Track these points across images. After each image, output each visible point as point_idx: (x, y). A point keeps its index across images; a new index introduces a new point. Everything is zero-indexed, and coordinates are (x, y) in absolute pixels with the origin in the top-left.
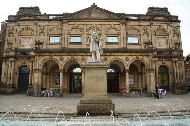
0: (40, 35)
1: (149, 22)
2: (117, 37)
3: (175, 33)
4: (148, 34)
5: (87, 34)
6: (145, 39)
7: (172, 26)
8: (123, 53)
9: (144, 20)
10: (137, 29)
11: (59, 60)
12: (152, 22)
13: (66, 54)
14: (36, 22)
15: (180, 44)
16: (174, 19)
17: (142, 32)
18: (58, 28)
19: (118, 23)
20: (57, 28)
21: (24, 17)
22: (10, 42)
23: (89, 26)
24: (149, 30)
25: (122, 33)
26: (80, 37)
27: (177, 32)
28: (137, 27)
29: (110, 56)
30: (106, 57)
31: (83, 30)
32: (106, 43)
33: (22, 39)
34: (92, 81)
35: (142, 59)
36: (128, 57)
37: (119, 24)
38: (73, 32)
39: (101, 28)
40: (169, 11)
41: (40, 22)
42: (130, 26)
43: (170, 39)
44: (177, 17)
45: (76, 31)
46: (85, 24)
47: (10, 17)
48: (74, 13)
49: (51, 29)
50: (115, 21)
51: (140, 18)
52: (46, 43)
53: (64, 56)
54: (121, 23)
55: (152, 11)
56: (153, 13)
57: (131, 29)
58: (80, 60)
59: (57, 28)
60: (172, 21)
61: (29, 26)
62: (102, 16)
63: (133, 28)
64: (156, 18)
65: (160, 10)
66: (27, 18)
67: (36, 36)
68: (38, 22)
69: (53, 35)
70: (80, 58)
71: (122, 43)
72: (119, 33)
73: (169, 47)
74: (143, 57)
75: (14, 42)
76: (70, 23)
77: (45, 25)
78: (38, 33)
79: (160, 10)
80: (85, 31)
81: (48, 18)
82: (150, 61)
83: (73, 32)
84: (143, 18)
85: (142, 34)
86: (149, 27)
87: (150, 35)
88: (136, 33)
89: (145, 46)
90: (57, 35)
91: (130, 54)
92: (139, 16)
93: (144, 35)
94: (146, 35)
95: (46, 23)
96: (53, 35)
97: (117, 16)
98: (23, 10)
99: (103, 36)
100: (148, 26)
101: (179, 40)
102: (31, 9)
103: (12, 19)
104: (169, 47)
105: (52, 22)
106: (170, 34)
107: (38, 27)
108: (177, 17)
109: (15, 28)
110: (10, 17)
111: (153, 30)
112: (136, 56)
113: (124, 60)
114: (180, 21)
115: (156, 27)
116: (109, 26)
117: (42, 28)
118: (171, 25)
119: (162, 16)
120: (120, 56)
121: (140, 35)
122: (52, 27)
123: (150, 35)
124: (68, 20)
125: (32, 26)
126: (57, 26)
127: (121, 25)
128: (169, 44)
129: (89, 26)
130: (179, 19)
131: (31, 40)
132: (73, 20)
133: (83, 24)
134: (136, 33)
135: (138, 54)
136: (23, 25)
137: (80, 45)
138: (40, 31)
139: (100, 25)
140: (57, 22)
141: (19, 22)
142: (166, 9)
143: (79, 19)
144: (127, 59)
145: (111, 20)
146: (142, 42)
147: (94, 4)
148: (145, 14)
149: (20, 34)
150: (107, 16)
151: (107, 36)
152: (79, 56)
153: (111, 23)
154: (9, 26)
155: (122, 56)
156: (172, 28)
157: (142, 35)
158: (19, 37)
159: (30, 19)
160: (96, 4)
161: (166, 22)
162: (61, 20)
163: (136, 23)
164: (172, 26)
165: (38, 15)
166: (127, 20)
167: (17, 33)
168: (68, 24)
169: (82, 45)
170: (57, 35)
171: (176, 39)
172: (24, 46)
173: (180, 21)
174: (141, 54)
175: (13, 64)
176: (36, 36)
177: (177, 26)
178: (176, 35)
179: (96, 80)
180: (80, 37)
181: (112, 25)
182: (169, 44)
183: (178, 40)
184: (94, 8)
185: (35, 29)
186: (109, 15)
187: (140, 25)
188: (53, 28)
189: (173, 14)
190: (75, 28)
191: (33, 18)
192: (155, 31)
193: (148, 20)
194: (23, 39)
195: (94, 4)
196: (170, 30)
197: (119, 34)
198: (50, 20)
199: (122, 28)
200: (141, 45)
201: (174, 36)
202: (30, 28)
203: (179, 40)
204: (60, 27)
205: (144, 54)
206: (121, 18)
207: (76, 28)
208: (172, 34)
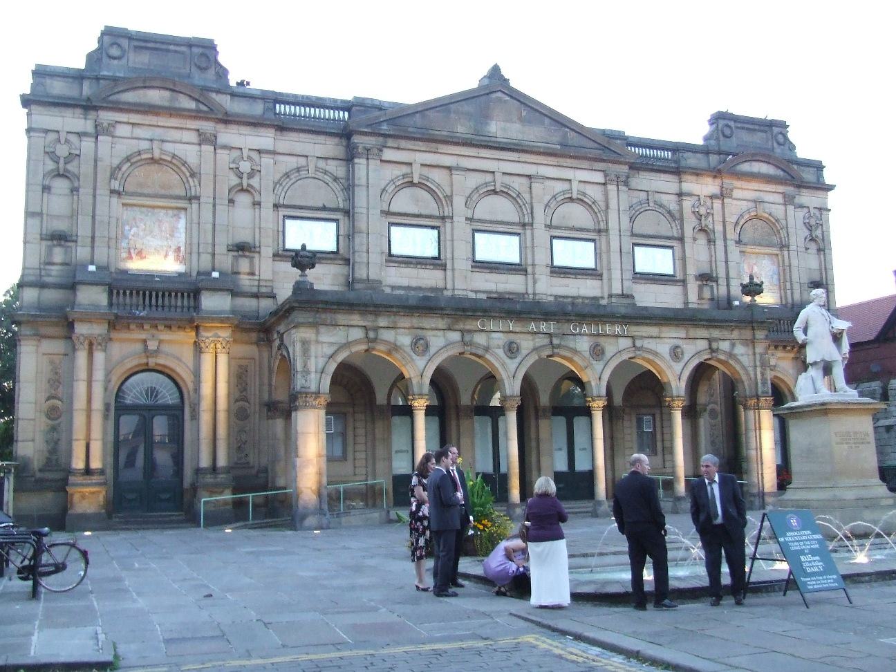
0: (231, 201)
1: (718, 181)
2: (593, 240)
3: (812, 240)
4: (712, 236)
5: (467, 219)
6: (698, 254)
7: (801, 206)
8: (664, 329)
9: (697, 173)
10: (669, 212)
11: (408, 349)
12: (728, 182)
13: (441, 323)
14: (207, 126)
15: (830, 288)
16: (808, 175)
17: (690, 223)
18: (325, 172)
19: (599, 178)
20: (320, 175)
21: (141, 92)
22: (61, 226)
23: (474, 180)
24: (718, 218)
25: (613, 224)
26: (436, 232)
27: (818, 233)
28: (670, 202)
29: (618, 336)
30: (602, 341)
31: (449, 198)
32: (549, 269)
33: (127, 214)
34: (846, 446)
35: (731, 355)
36: (680, 342)
37: (602, 181)
38: (404, 202)
39: (527, 196)
40: (792, 136)
41: (233, 129)
42: (643, 196)
43: (794, 262)
44: (818, 167)
45: (416, 201)
46: (458, 168)
47: (40, 73)
48: (416, 105)
49: (287, 175)
50: (586, 164)
51: (673, 160)
52: (267, 252)
53: (430, 333)
54: (613, 177)
55: (727, 132)
56: (734, 139)
57: (646, 207)
58: (500, 352)
59: (320, 175)
60: (801, 185)
61: (169, 147)
62: (533, 134)
63: (661, 206)
64: (745, 167)
65: (757, 127)
66: (155, 96)
67: (214, 206)
68: (220, 127)
69: (301, 208)
70: (501, 343)
71: (616, 274)
72: (602, 226)
73: (790, 300)
74: (733, 345)
75: (84, 231)
76: (388, 154)
77: (259, 151)
78: (224, 193)
79: (757, 127)
80: (459, 201)
81: (274, 113)
82: (758, 363)
83: (404, 202)
84: (692, 160)
85: (688, 233)
86: (717, 204)
87: (720, 243)
88: (665, 228)
89: (700, 288)
90: (324, 208)
91: (687, 333)
92: (676, 148)
93: (695, 239)
94: (702, 240)
95: (265, 139)
96: (301, 208)
97: (596, 145)
98: (125, 43)
99: (536, 233)
100: (711, 197)
101: (826, 269)
102: (172, 47)
103: (58, 88)
104: (790, 300)
105: (293, 136)
106: (792, 240)
107: (223, 156)
108: (818, 167)
109: (87, 145)
110: (40, 73)
111: (731, 219)
112: (710, 341)
113: (667, 357)
114: (830, 188)
115: (744, 205)
116: (559, 187)
117: (245, 167)
118: (798, 200)
119: (766, 158)
120: (650, 340)
121: (681, 239)
122: (293, 162)
123: (720, 243)
124: (381, 139)
125: (181, 141)
126: (321, 164)
127: (612, 188)
128: (788, 285)
129: (474, 180)
130: (828, 178)
131: (182, 224)
132: (403, 143)
133: (449, 168)
134: (665, 228)
135: (716, 333)
136: (129, 135)
137: (438, 274)
138: (234, 180)
139: (524, 181)
140: (321, 138)
141: (106, 117)
142: (783, 125)
143: (431, 139)
144: (676, 353)
145: (569, 162)
146: (692, 271)
147: (495, 70)
148: (700, 142)
149: (115, 185)
150: (556, 139)
151: (553, 237)
152: (494, 335)
153: (568, 174)
154: (47, 131)
155: (658, 340)
156: (801, 214)
157: (688, 239)
158: (115, 199)
159: (177, 105)
160: (506, 73)
161: (781, 189)
162: (345, 134)
163: (665, 183)
164: (801, 206)
165: (218, 92)
166: (638, 166)
167: (103, 175)
168: (381, 161)
169: (449, 273)
170: (324, 208)
171: (812, 262)
172: (140, 254)
173: (830, 188)
174: (726, 334)
175: (99, 357)
176: (214, 206)
177: (820, 209)
178: (813, 246)
179: (855, 443)
180: (436, 232)
181: (575, 186)
182: (788, 285)
183: (820, 270)
184: (499, 94)
185: (207, 169)
186: (565, 135)
187: (680, 195)
188: (298, 170)
189: (802, 153)
190: (411, 184)
191: (192, 105)
192: (737, 223)
193: (716, 173)
194: (136, 213)
195: (495, 70)
196: (795, 219)
197: (599, 231)
198: (282, 127)
199: (613, 204)
200: (684, 282)
201: (807, 249)
202: (174, 156)
203: (826, 269)
204: (333, 167)
205: (736, 334)
206: (610, 152)
207: (419, 185)
208: (801, 242)
